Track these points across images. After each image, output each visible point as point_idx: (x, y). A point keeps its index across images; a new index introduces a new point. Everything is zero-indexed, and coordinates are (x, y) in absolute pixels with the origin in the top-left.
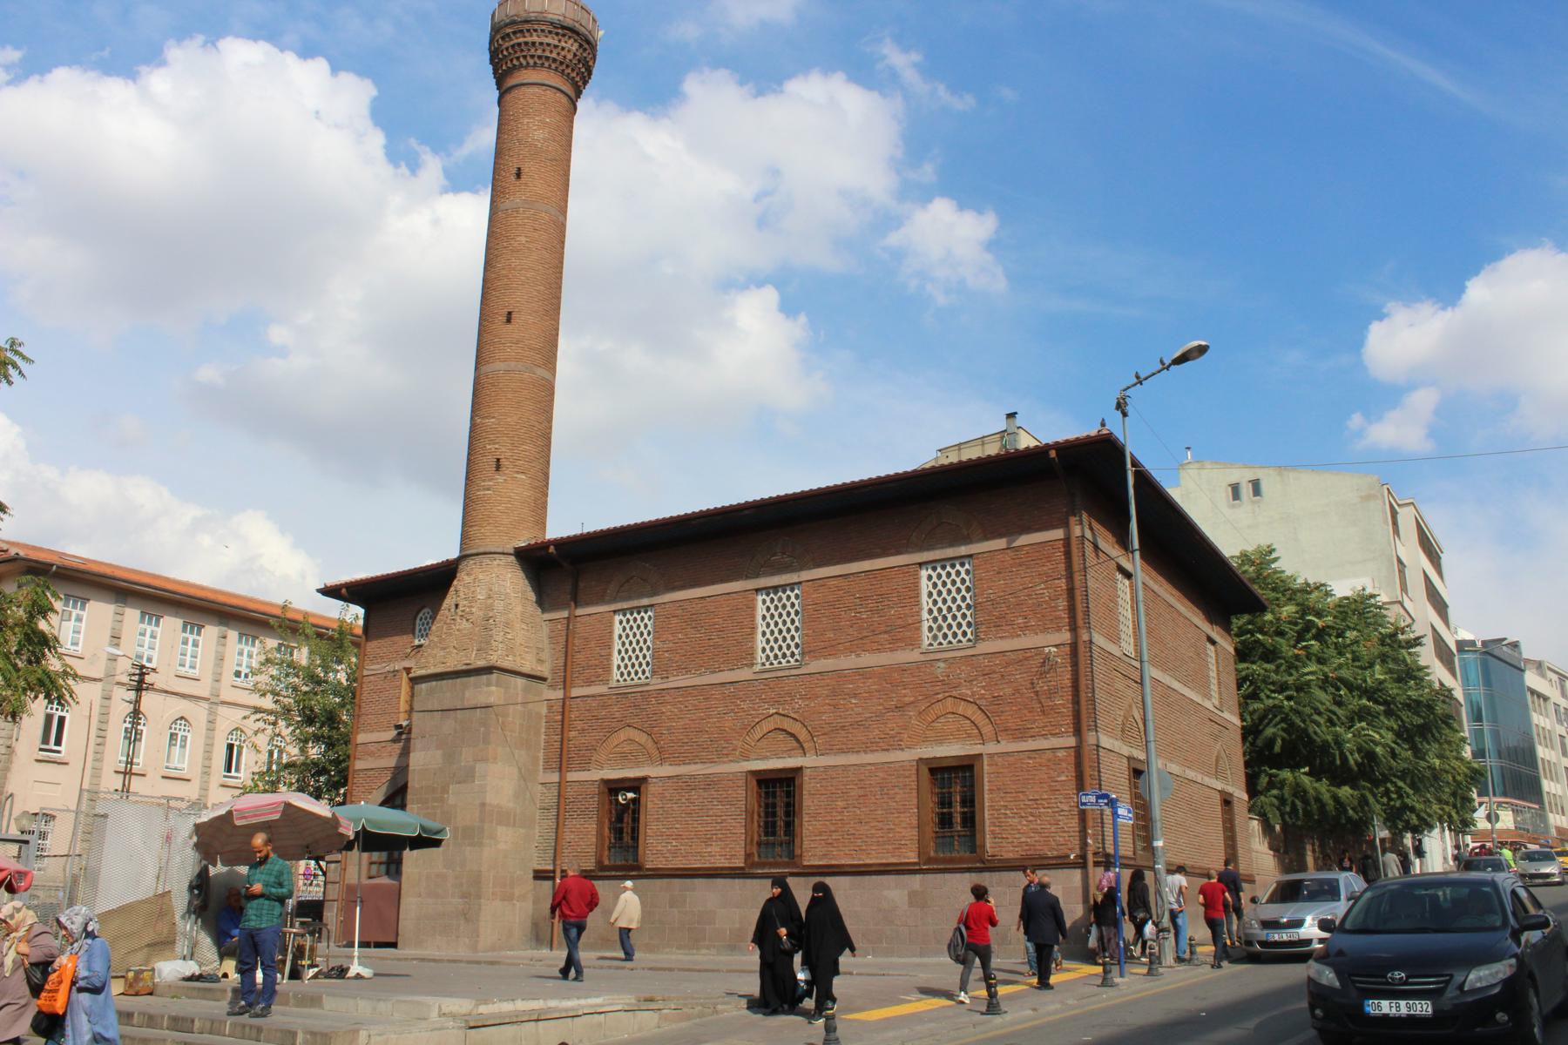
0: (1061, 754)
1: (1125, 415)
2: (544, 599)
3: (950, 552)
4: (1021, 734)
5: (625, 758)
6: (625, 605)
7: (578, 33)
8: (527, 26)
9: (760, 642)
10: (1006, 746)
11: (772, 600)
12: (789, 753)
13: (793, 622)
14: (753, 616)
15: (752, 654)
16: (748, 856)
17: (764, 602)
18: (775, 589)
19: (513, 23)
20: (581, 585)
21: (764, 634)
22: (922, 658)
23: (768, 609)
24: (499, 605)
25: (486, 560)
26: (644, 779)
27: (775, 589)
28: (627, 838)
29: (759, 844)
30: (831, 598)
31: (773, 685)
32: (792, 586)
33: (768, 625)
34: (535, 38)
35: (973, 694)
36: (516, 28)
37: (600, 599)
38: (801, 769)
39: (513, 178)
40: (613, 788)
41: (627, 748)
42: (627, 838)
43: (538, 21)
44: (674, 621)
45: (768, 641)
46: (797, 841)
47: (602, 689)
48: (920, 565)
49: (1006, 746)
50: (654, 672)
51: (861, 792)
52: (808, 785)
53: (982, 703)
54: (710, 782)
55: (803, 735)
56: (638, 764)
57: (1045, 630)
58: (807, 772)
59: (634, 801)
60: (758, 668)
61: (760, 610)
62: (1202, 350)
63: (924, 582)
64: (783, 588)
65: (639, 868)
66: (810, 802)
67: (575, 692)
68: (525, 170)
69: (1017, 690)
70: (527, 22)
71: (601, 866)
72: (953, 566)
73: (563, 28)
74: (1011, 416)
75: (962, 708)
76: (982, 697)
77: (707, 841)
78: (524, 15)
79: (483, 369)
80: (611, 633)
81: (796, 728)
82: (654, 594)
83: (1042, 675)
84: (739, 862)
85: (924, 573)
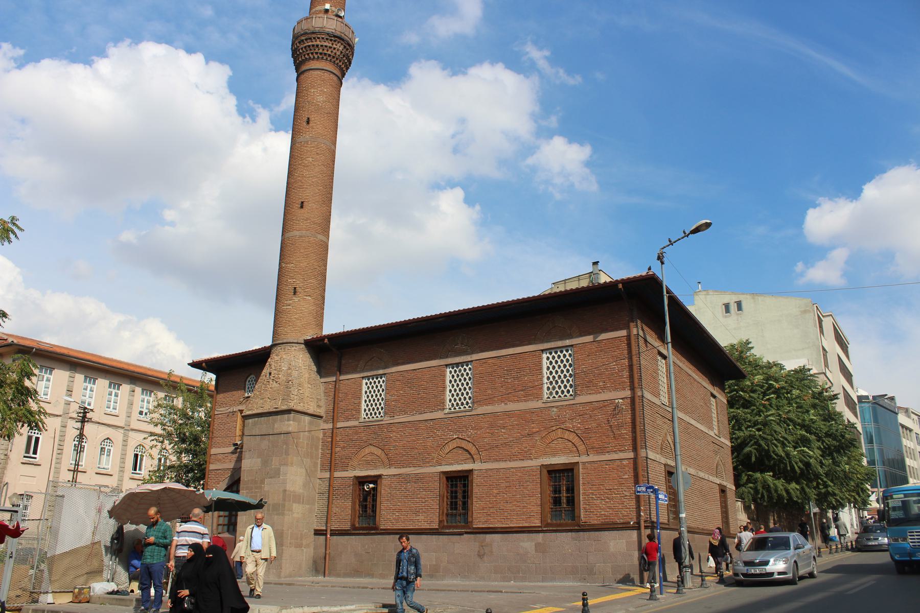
1: (662, 263)
2: (322, 371)
3: (560, 343)
4: (601, 450)
5: (368, 464)
6: (369, 374)
7: (343, 40)
8: (314, 36)
9: (448, 396)
11: (455, 371)
12: (465, 461)
13: (467, 384)
14: (444, 381)
15: (443, 403)
16: (440, 522)
17: (451, 372)
18: (457, 365)
19: (306, 34)
20: (343, 362)
21: (450, 391)
22: (543, 405)
23: (453, 376)
24: (295, 374)
25: (288, 347)
26: (380, 476)
27: (457, 365)
28: (369, 511)
29: (447, 515)
30: (490, 370)
31: (455, 421)
32: (467, 363)
33: (453, 386)
34: (318, 43)
36: (307, 37)
37: (355, 371)
38: (472, 470)
39: (305, 124)
40: (361, 481)
41: (370, 458)
42: (369, 511)
43: (320, 33)
44: (398, 383)
45: (453, 395)
46: (470, 513)
47: (355, 423)
48: (542, 351)
50: (385, 413)
52: (476, 480)
53: (579, 432)
54: (418, 478)
56: (376, 467)
57: (616, 389)
58: (475, 473)
59: (373, 489)
60: (447, 411)
61: (448, 377)
62: (708, 225)
63: (545, 360)
64: (462, 364)
65: (376, 528)
66: (477, 490)
67: (339, 425)
68: (312, 119)
69: (599, 425)
70: (313, 33)
71: (354, 527)
72: (562, 352)
73: (335, 36)
74: (595, 263)
75: (567, 435)
76: (579, 428)
77: (417, 513)
78: (312, 29)
79: (287, 235)
80: (361, 390)
81: (469, 447)
82: (386, 367)
83: (614, 415)
84: (435, 526)
85: (545, 356)
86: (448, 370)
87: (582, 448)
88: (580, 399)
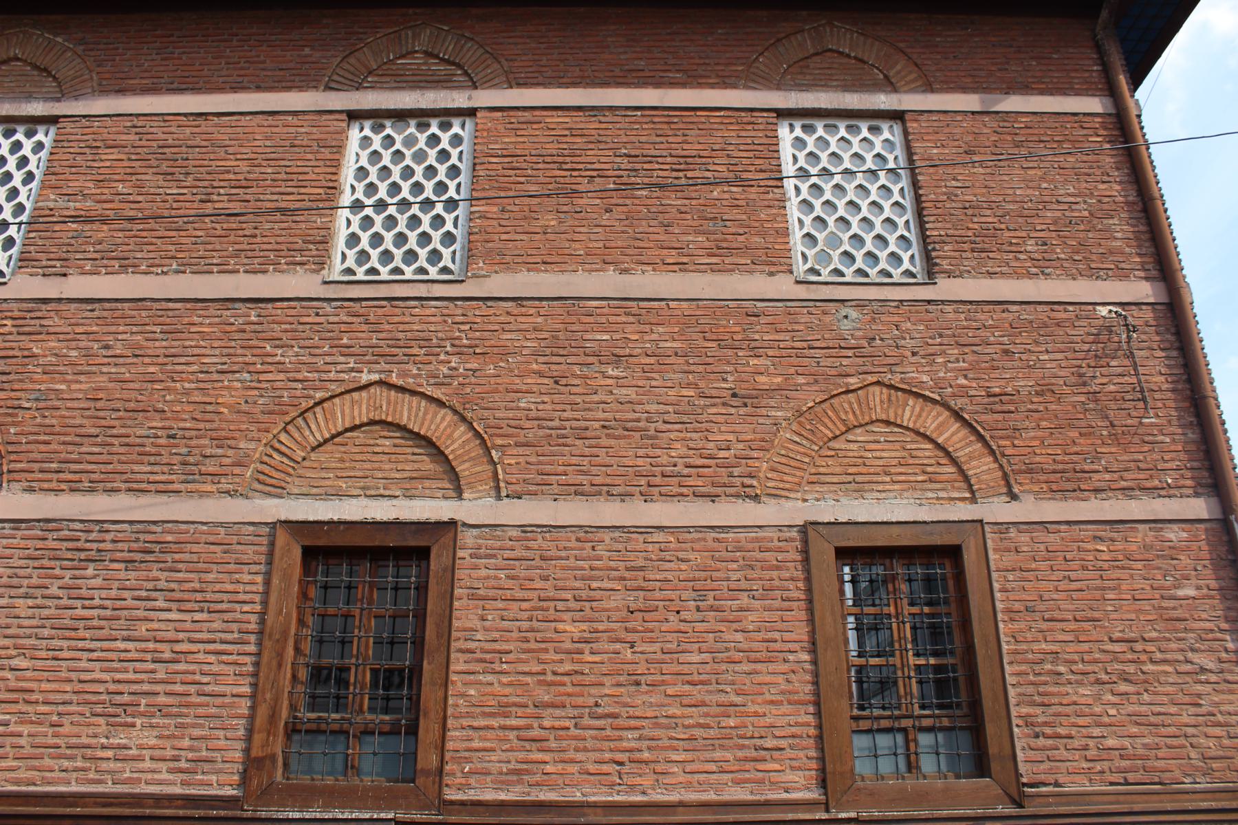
0: (1174, 534)
3: (853, 101)
4: (1069, 481)
9: (344, 223)
10: (1029, 509)
11: (389, 141)
15: (324, 242)
16: (252, 765)
17: (366, 141)
18: (400, 116)
22: (802, 292)
27: (400, 116)
29: (292, 730)
30: (552, 148)
31: (373, 319)
35: (938, 385)
38: (451, 525)
49: (1029, 509)
51: (635, 600)
52: (472, 571)
54: (150, 546)
55: (456, 441)
58: (468, 537)
66: (475, 618)
69: (1045, 389)
75: (909, 412)
76: (963, 392)
77: (118, 712)
81: (437, 424)
86: (355, 134)
87: (982, 467)
88: (946, 288)
